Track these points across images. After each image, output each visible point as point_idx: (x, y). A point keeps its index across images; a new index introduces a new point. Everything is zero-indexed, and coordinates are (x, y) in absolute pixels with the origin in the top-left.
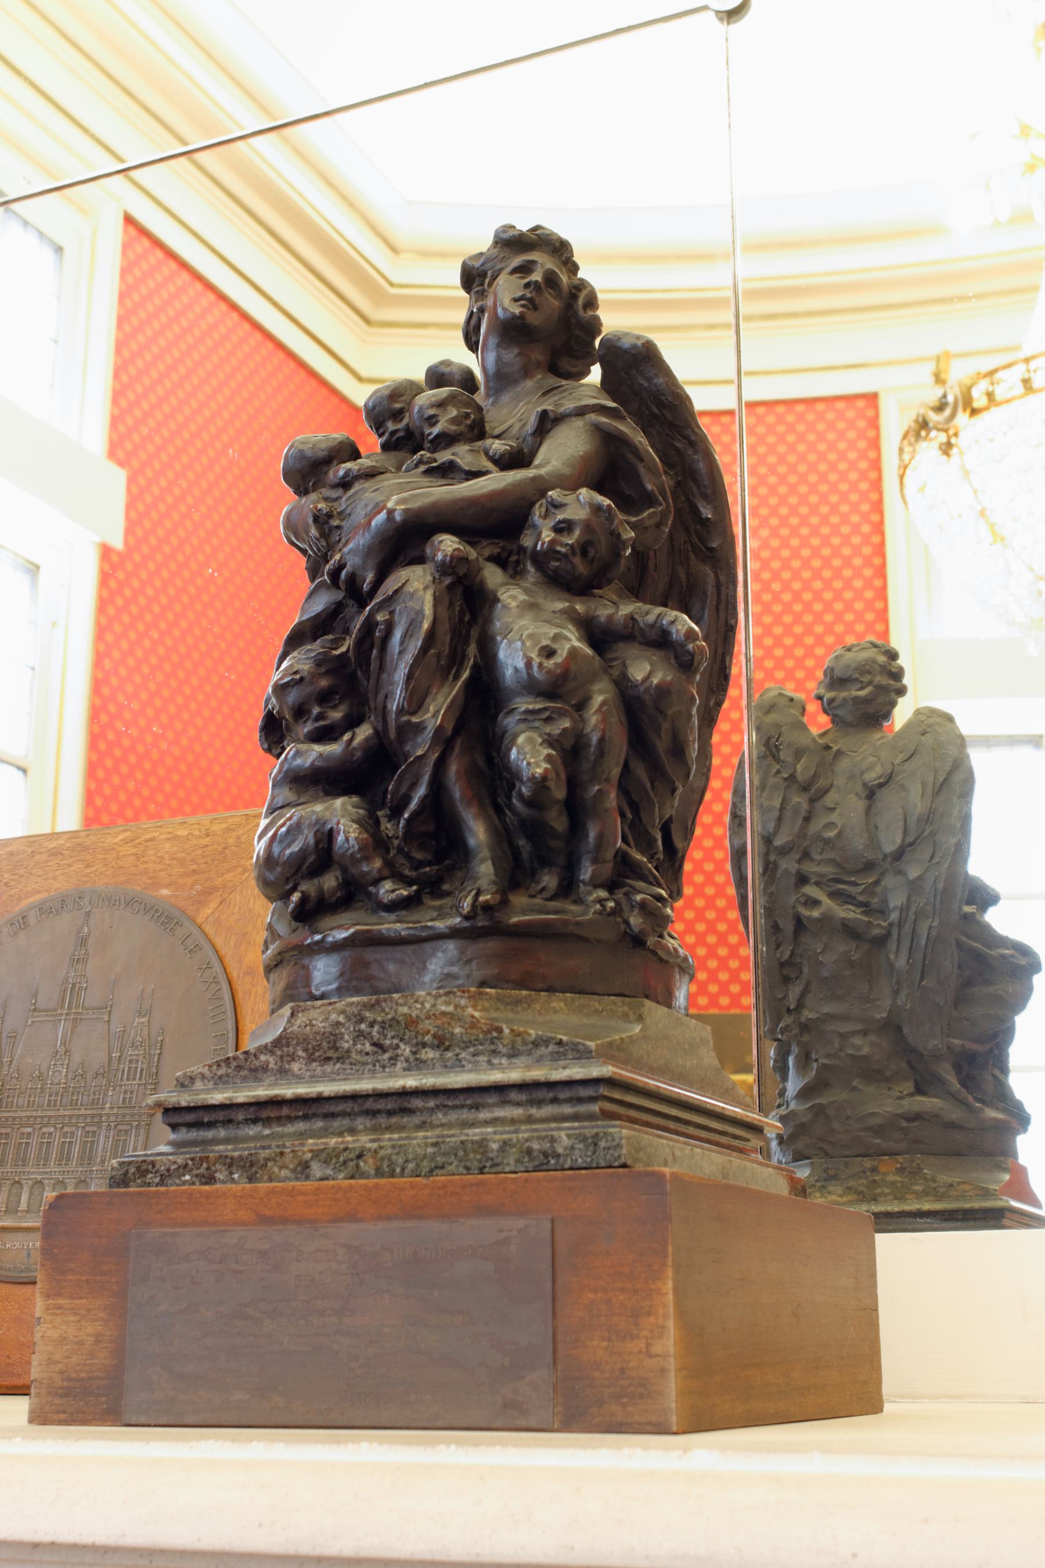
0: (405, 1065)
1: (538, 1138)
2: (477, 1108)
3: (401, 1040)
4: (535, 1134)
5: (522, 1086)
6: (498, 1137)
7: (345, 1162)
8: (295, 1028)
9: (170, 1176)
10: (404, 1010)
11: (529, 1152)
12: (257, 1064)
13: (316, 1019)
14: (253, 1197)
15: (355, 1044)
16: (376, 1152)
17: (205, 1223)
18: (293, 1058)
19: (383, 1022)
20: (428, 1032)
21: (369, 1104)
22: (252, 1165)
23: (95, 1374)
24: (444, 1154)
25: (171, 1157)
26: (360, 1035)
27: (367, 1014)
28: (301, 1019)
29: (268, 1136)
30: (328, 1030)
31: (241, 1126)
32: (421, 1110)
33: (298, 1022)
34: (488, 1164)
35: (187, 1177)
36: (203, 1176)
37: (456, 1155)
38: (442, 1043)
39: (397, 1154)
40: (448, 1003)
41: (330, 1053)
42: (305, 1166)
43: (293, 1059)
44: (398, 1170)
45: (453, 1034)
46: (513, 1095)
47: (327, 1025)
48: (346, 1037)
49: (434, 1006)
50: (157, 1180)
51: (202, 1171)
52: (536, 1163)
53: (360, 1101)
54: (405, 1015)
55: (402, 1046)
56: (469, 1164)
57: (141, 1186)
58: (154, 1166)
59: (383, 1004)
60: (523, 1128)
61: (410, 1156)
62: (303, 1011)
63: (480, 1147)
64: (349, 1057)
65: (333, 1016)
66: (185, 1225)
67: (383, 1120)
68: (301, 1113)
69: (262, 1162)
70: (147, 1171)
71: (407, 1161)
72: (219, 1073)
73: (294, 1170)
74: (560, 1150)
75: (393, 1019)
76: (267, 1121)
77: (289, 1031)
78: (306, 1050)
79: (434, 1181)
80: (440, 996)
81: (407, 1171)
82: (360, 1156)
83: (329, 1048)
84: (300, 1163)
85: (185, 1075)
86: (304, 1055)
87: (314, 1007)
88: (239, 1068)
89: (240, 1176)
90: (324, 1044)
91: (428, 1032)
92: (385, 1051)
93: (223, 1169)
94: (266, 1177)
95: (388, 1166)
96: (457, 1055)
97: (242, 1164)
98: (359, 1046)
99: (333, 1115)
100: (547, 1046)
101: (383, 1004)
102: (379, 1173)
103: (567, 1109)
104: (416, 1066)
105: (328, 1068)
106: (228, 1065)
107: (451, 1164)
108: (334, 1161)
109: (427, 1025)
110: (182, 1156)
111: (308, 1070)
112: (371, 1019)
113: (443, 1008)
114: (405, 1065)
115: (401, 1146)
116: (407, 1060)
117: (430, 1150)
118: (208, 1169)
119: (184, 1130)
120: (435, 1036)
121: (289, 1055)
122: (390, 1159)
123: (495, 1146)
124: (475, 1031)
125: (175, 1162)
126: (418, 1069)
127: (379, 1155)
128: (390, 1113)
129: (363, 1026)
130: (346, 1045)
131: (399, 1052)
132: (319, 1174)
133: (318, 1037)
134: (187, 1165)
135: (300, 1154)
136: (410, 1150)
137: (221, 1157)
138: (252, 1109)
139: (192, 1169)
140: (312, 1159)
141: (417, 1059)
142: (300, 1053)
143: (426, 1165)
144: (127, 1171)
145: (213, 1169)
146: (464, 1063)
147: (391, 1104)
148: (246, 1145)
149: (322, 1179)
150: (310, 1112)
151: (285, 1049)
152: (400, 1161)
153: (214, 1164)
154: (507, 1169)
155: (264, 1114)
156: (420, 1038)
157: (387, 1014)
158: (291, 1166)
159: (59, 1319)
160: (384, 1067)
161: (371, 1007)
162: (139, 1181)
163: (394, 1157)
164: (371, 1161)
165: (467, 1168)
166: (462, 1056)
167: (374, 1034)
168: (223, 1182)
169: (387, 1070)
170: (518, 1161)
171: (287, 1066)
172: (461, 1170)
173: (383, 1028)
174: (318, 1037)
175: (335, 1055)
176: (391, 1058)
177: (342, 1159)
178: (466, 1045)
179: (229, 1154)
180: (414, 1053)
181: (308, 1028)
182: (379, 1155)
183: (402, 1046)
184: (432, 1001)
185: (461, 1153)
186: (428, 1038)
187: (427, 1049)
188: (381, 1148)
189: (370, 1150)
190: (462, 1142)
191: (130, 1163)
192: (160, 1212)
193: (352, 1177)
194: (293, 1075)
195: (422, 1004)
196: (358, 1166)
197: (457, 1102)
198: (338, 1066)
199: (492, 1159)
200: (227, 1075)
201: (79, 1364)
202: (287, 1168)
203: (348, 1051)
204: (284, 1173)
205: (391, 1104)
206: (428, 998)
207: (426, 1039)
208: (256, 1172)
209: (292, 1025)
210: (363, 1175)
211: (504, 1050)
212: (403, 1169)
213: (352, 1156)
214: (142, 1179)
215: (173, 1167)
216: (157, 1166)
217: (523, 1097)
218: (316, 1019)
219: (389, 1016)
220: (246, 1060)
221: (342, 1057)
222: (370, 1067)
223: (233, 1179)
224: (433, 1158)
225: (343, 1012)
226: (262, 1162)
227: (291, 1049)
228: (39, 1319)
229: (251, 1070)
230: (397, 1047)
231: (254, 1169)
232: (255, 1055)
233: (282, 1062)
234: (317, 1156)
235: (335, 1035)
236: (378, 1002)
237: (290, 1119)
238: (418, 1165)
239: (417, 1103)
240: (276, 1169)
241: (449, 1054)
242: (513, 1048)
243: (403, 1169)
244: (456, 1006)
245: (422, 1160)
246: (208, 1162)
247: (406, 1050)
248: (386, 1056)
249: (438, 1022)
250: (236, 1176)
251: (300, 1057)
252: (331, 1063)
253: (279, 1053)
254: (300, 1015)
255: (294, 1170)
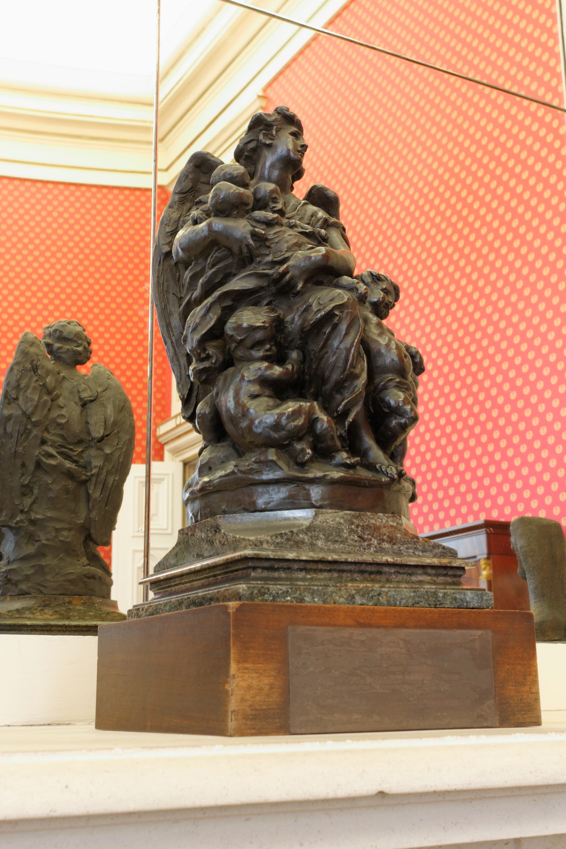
0: (375, 549)
1: (459, 593)
2: (411, 575)
3: (372, 536)
4: (457, 591)
5: (433, 567)
6: (442, 591)
7: (372, 597)
8: (318, 522)
9: (278, 597)
10: (373, 521)
11: (455, 599)
12: (298, 539)
13: (329, 519)
14: (353, 612)
15: (349, 535)
16: (387, 593)
17: (328, 625)
18: (318, 538)
19: (363, 526)
20: (385, 534)
21: (363, 567)
22: (324, 594)
23: (271, 707)
24: (419, 597)
25: (278, 586)
26: (352, 531)
27: (355, 521)
28: (321, 518)
29: (308, 579)
30: (335, 526)
31: (293, 571)
32: (385, 573)
33: (319, 519)
34: (438, 603)
35: (289, 598)
36: (297, 598)
37: (424, 598)
38: (392, 540)
39: (397, 595)
40: (393, 521)
41: (337, 538)
42: (353, 597)
43: (318, 539)
44: (398, 603)
45: (396, 537)
46: (429, 571)
47: (335, 523)
48: (345, 531)
49: (387, 521)
50: (271, 598)
51: (296, 595)
52: (459, 604)
53: (358, 565)
54: (373, 524)
55: (373, 540)
56: (430, 602)
57: (261, 601)
58: (269, 591)
59: (363, 517)
60: (448, 587)
61: (403, 597)
62: (321, 514)
63: (435, 595)
64: (347, 542)
65: (338, 519)
66: (317, 625)
67: (366, 575)
68: (328, 568)
69: (330, 593)
70: (265, 593)
71: (402, 599)
72: (277, 541)
73: (347, 599)
74: (468, 599)
75: (367, 525)
76: (307, 570)
77: (315, 523)
78: (324, 535)
79: (440, 610)
80: (390, 517)
81: (402, 604)
82: (379, 594)
83: (336, 536)
84: (350, 596)
85: (257, 539)
86: (323, 537)
87: (327, 513)
88: (288, 540)
89: (319, 600)
90: (334, 533)
91: (385, 534)
92: (364, 540)
93: (309, 595)
94: (332, 601)
95: (393, 600)
96: (399, 548)
97: (319, 593)
98: (352, 537)
99: (343, 571)
100: (439, 549)
101: (363, 517)
102: (389, 604)
103: (449, 579)
104: (380, 550)
105: (337, 546)
106: (282, 537)
107: (422, 602)
108: (367, 596)
109: (384, 530)
110: (284, 587)
111: (326, 546)
112: (357, 524)
113: (391, 523)
114: (375, 549)
115: (398, 591)
116: (376, 547)
117: (412, 594)
118: (300, 594)
119: (260, 571)
120: (388, 537)
121: (315, 536)
122: (394, 597)
123: (441, 595)
124: (407, 537)
125: (281, 590)
126: (382, 552)
127: (389, 595)
128: (371, 573)
129: (353, 527)
130: (345, 535)
131: (372, 542)
132: (359, 602)
133: (331, 529)
134: (288, 591)
135: (349, 590)
136: (403, 593)
137: (307, 588)
138: (302, 563)
139: (291, 594)
140: (356, 593)
141: (381, 547)
142: (321, 536)
143: (411, 602)
144: (253, 592)
145: (303, 594)
146: (403, 552)
147: (373, 569)
148: (315, 583)
149: (361, 605)
150: (333, 568)
151: (313, 533)
152: (399, 598)
153: (304, 592)
154: (446, 606)
155: (309, 566)
156: (381, 537)
157: (365, 522)
158: (345, 597)
159: (246, 676)
160: (365, 549)
161: (357, 517)
162: (260, 598)
163: (396, 596)
164: (385, 597)
165: (429, 604)
166: (401, 548)
167: (359, 531)
168: (309, 602)
169: (366, 551)
170: (451, 603)
171: (315, 542)
172: (427, 605)
173: (363, 529)
174: (331, 529)
175: (340, 540)
176: (368, 545)
177: (371, 595)
178: (403, 543)
179: (312, 587)
180: (379, 544)
181: (325, 523)
182: (389, 595)
183: (373, 540)
184: (386, 519)
185: (426, 597)
186: (385, 537)
187: (385, 543)
188: (389, 591)
189: (384, 592)
190: (426, 592)
191: (254, 588)
192: (303, 617)
193: (376, 605)
194: (318, 547)
195: (381, 519)
196: (379, 599)
197: (404, 571)
198: (341, 545)
199: (440, 601)
200: (282, 543)
201: (261, 701)
202: (343, 597)
203: (346, 538)
204: (342, 600)
205: (373, 569)
206: (384, 517)
207: (384, 537)
208: (327, 599)
209: (316, 521)
210: (382, 604)
211: (420, 548)
212: (400, 603)
213: (376, 594)
214: (262, 597)
215: (280, 592)
216: (271, 591)
217: (433, 572)
218: (329, 519)
219: (366, 524)
220: (292, 536)
221: (344, 541)
222: (358, 548)
223: (315, 601)
224: (414, 598)
225: (343, 518)
226: (330, 593)
227: (316, 533)
228: (234, 675)
229: (294, 541)
230: (371, 540)
231: (326, 597)
232: (297, 534)
233: (312, 539)
234: (358, 592)
235: (339, 529)
236: (360, 515)
237: (321, 571)
238: (407, 601)
239: (386, 569)
240: (337, 598)
241: (396, 547)
242: (424, 548)
243: (400, 603)
244: (397, 524)
245: (409, 599)
246: (300, 591)
247: (375, 542)
248: (366, 543)
249: (389, 530)
250: (316, 600)
251: (321, 538)
252: (338, 543)
253: (310, 534)
254: (320, 515)
255: (347, 599)
